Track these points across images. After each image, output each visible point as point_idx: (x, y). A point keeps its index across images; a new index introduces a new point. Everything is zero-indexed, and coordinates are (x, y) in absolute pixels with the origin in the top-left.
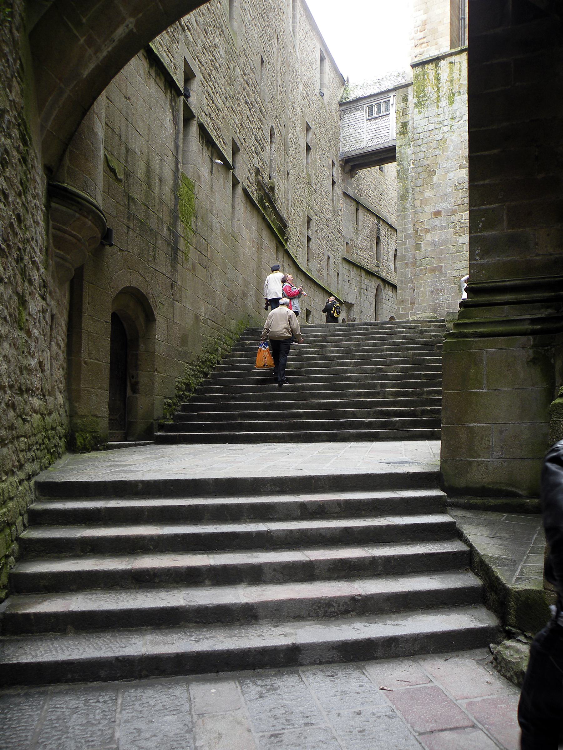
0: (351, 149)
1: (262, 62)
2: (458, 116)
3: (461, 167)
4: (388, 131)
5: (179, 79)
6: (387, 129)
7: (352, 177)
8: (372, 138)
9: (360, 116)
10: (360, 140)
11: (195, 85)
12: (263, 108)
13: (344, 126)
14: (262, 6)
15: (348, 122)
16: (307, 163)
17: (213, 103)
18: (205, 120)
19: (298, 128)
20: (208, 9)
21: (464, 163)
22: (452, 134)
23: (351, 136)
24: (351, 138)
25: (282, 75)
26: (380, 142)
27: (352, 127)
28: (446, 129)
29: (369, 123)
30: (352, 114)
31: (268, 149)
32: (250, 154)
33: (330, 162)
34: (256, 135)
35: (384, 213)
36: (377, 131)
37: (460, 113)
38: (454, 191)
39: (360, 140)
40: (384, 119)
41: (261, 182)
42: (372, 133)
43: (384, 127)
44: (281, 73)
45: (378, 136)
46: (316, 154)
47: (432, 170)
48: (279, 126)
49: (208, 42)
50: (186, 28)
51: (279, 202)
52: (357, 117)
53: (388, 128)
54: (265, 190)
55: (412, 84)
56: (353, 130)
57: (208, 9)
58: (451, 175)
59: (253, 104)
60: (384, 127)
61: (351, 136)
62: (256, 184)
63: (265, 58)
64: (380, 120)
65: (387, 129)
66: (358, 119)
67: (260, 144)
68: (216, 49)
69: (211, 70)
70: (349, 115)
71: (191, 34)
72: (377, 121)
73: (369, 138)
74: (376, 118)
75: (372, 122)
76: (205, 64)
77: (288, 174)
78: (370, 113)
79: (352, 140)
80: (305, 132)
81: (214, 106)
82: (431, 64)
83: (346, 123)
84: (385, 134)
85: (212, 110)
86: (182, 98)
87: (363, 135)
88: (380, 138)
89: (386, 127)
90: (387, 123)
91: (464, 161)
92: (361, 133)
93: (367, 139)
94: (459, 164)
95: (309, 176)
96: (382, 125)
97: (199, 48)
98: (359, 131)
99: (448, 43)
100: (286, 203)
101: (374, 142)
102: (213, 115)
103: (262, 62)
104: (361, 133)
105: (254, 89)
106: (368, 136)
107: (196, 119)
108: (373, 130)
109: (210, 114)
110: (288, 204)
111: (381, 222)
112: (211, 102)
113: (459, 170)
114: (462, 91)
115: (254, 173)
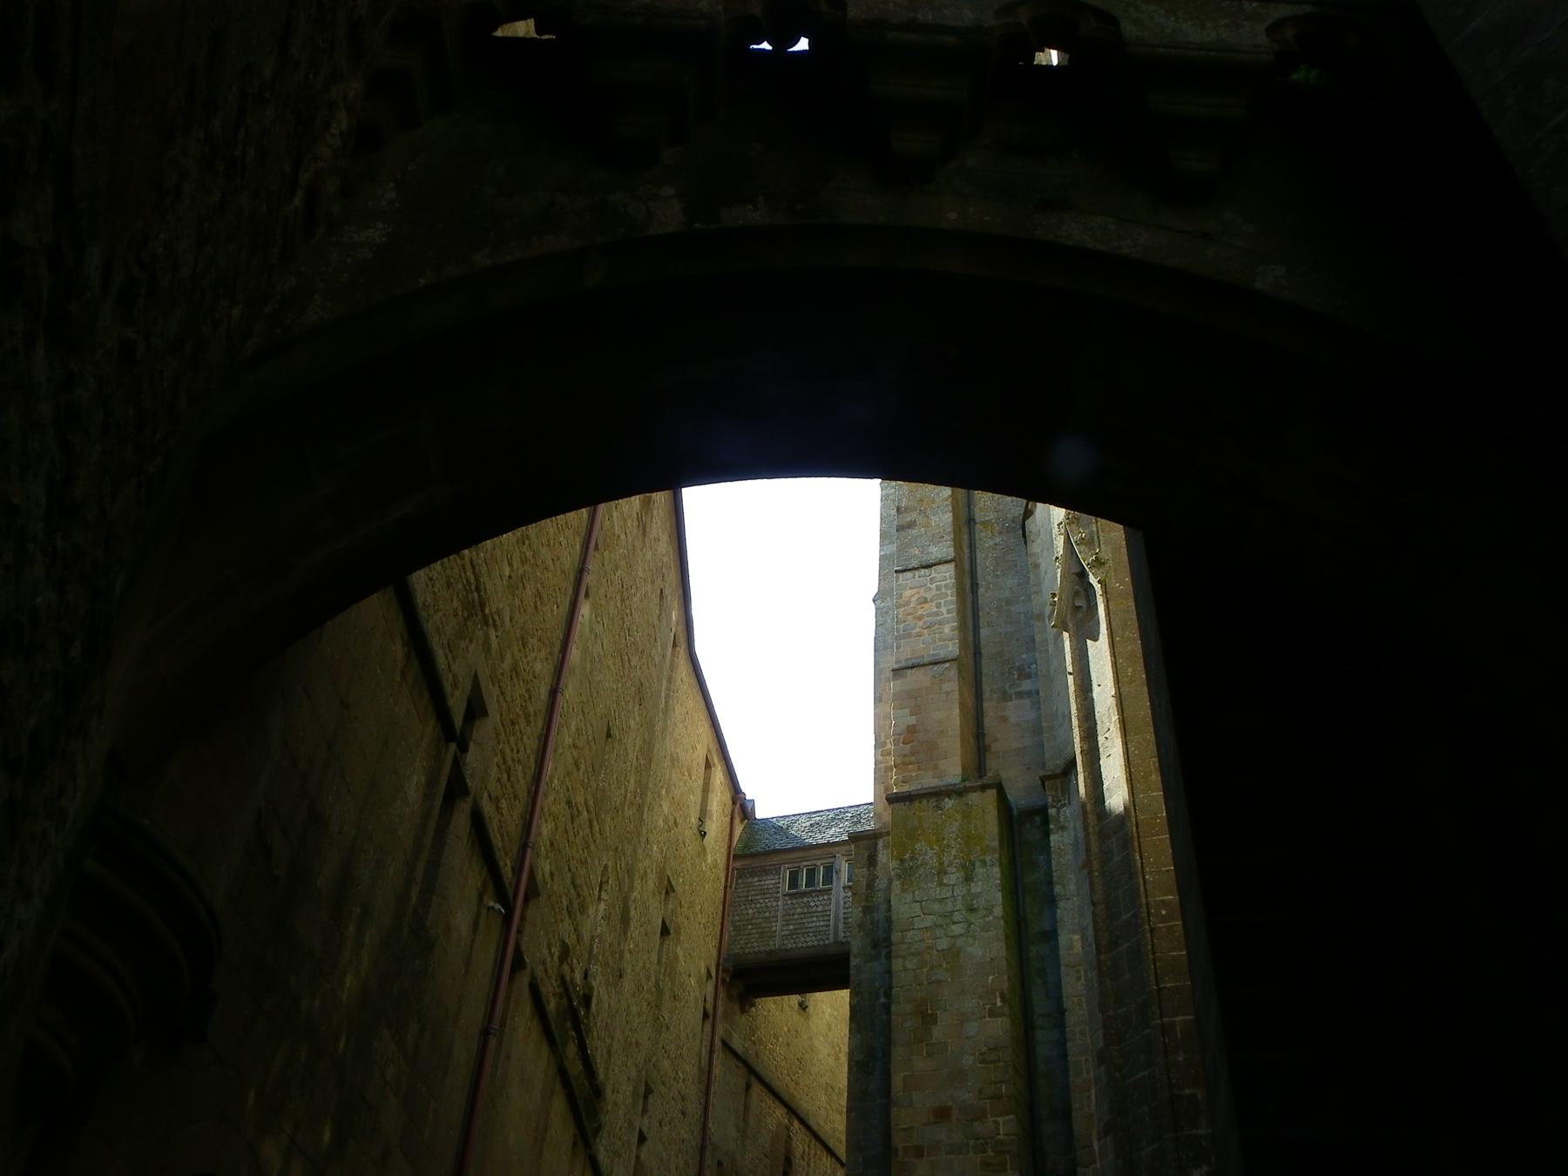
0: (747, 950)
1: (609, 735)
2: (981, 908)
3: (993, 1013)
4: (827, 923)
5: (457, 704)
6: (826, 918)
7: (743, 1011)
11: (484, 730)
12: (595, 823)
13: (737, 899)
14: (623, 641)
15: (745, 894)
16: (659, 962)
17: (509, 780)
18: (487, 808)
19: (651, 883)
20: (536, 607)
21: (999, 1004)
22: (971, 940)
25: (638, 772)
27: (754, 905)
28: (957, 929)
30: (756, 879)
31: (591, 911)
32: (557, 910)
33: (703, 971)
34: (574, 874)
35: (804, 1104)
36: (804, 921)
37: (986, 901)
38: (979, 1065)
39: (769, 934)
40: (821, 898)
41: (568, 978)
42: (794, 922)
43: (818, 914)
44: (636, 768)
46: (679, 948)
47: (930, 1012)
48: (619, 869)
49: (522, 662)
50: (491, 622)
51: (595, 1033)
52: (765, 887)
54: (570, 1000)
55: (888, 833)
56: (755, 910)
57: (536, 607)
58: (972, 1028)
59: (580, 809)
60: (818, 914)
62: (556, 981)
63: (615, 732)
64: (810, 899)
65: (826, 918)
67: (578, 895)
68: (534, 680)
69: (518, 715)
70: (750, 880)
71: (497, 637)
72: (805, 900)
73: (788, 933)
74: (804, 894)
75: (794, 901)
76: (509, 699)
77: (621, 976)
78: (794, 882)
80: (663, 896)
81: (508, 785)
82: (924, 802)
83: (741, 895)
84: (821, 929)
85: (504, 794)
86: (453, 746)
87: (774, 924)
88: (811, 935)
89: (824, 914)
90: (827, 908)
91: (999, 1000)
93: (783, 933)
94: (988, 1007)
95: (660, 992)
97: (506, 665)
98: (767, 914)
99: (958, 770)
100: (608, 1041)
101: (797, 940)
102: (504, 804)
103: (609, 735)
105: (586, 780)
106: (785, 928)
107: (470, 800)
108: (796, 917)
109: (498, 800)
110: (611, 1045)
111: (796, 1123)
112: (506, 776)
113: (987, 1018)
114: (988, 858)
115: (557, 954)
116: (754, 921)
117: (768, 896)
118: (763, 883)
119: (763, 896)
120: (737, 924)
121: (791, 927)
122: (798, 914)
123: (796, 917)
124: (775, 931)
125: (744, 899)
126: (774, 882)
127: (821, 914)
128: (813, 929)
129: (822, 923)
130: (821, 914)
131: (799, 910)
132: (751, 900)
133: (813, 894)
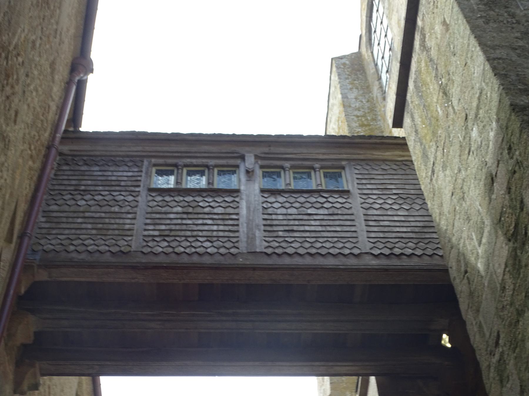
0: (72, 248)
6: (231, 222)
8: (167, 233)
9: (125, 179)
10: (117, 232)
15: (74, 182)
23: (81, 215)
24: (80, 220)
26: (201, 250)
29: (159, 198)
30: (97, 168)
40: (219, 199)
42: (168, 222)
45: (195, 233)
52: (114, 178)
53: (235, 222)
61: (81, 215)
64: (198, 199)
65: (231, 222)
66: (113, 183)
72: (189, 199)
73: (156, 233)
75: (168, 199)
79: (84, 226)
84: (221, 234)
89: (227, 217)
92: (124, 216)
93: (146, 233)
96: (207, 210)
98: (116, 209)
104: (124, 216)
106: (151, 227)
108: (172, 216)
116: (87, 214)
117: (117, 188)
118: (110, 173)
119: (107, 188)
120: (55, 214)
121: (163, 227)
122: (177, 213)
123: (172, 216)
124: (129, 230)
125: (72, 188)
126: (130, 174)
127: (220, 217)
128: (205, 233)
129: (221, 228)
130: (220, 217)
131: (179, 209)
132: (84, 191)
133: (205, 194)
